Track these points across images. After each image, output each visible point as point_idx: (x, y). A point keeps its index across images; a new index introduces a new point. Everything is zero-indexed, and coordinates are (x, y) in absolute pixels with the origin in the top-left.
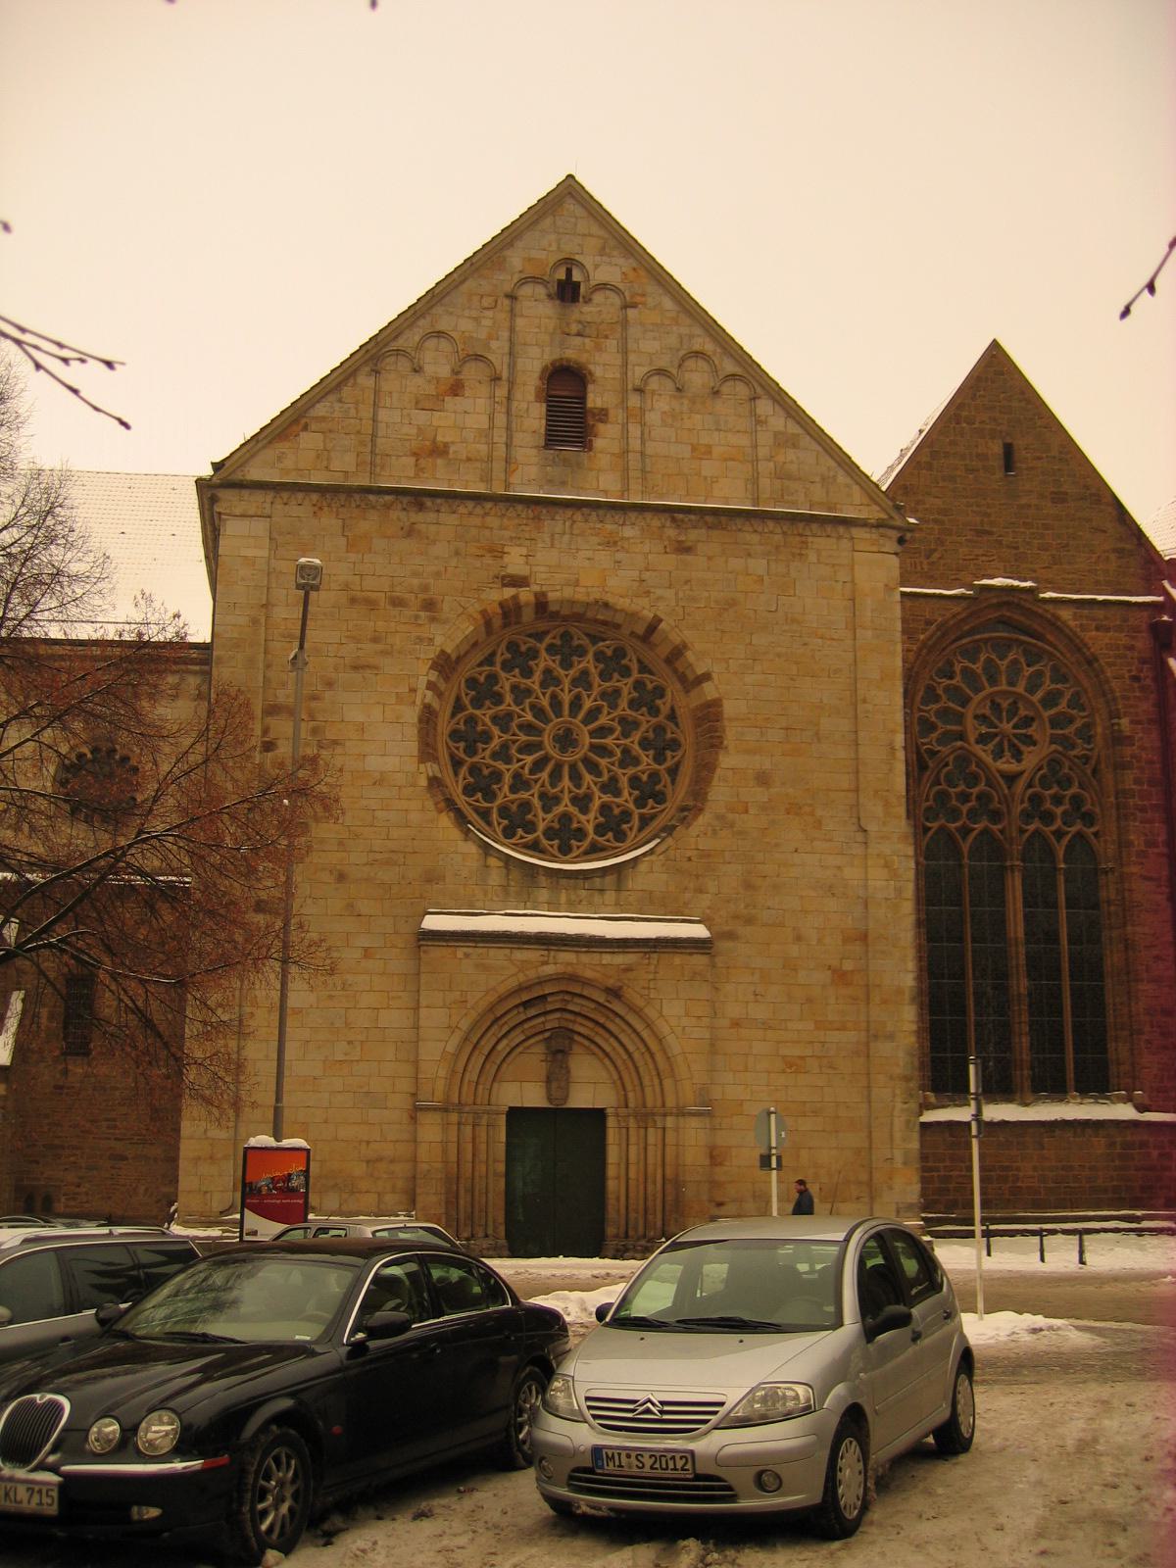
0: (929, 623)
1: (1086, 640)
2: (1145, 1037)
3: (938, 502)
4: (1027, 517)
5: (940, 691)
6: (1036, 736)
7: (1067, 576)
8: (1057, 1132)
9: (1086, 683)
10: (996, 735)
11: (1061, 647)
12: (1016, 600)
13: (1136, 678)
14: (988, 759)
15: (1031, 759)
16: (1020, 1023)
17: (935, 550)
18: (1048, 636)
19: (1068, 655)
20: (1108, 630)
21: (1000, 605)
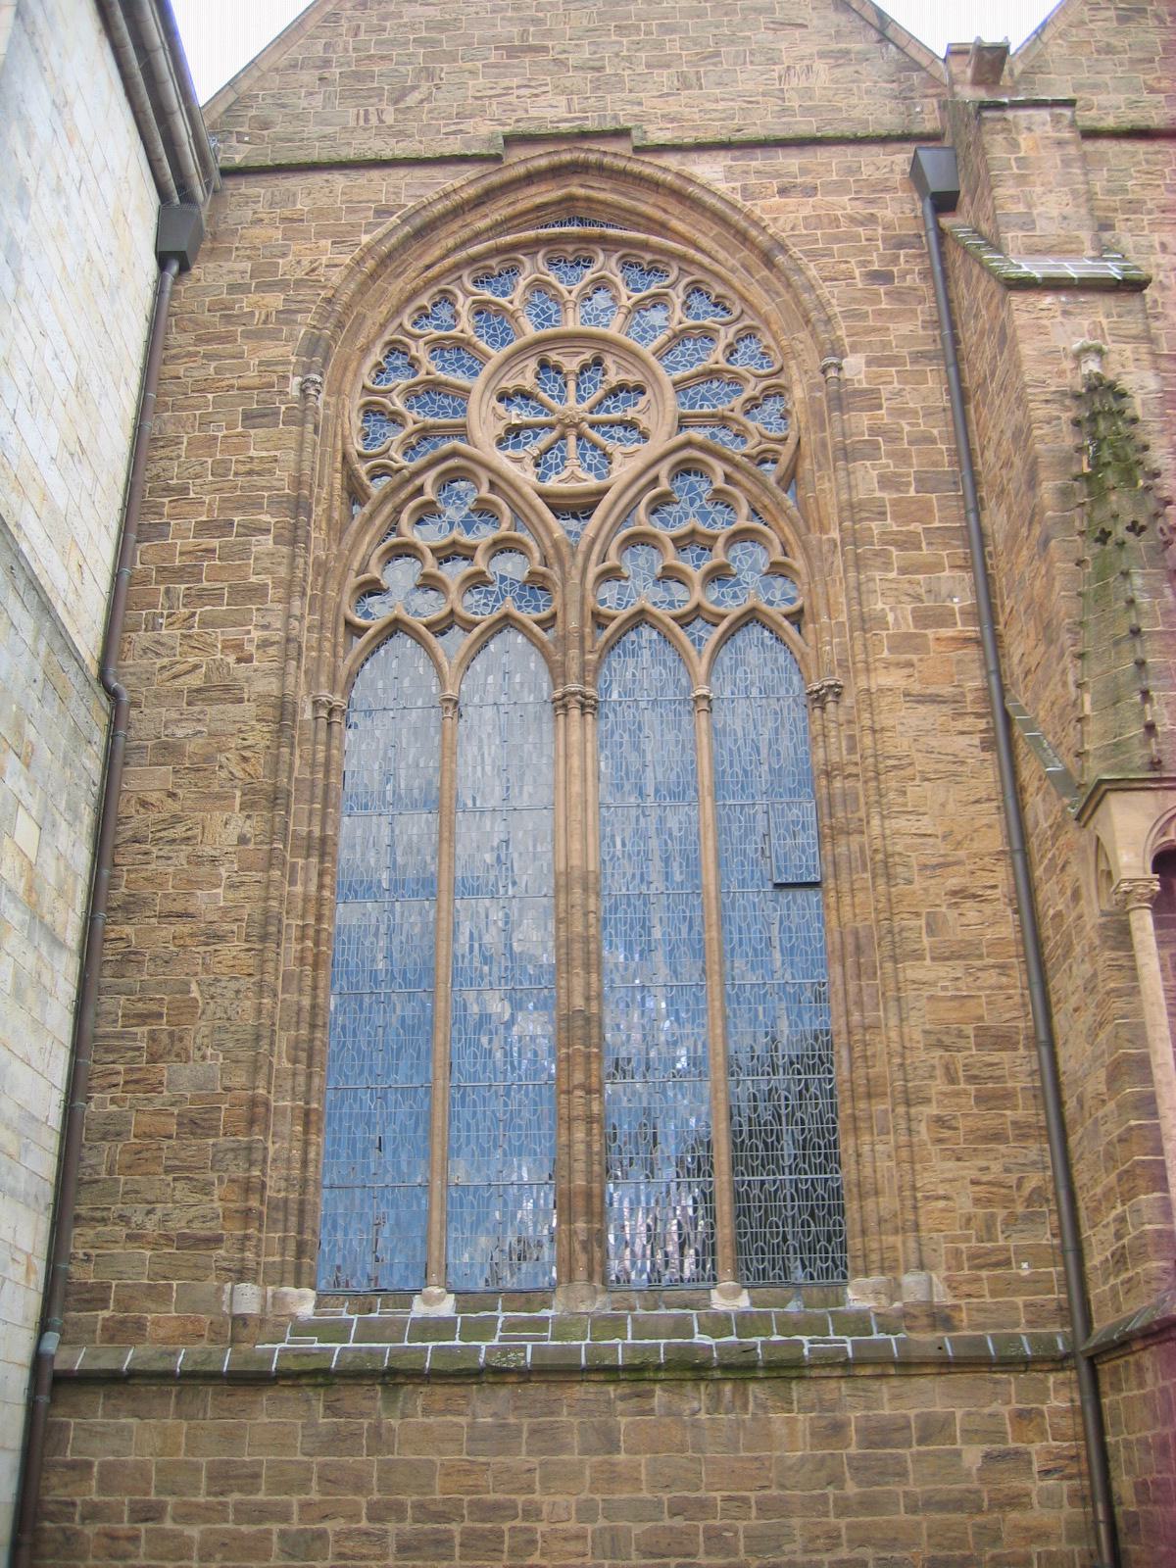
0: (383, 212)
1: (758, 212)
2: (933, 1110)
3: (430, 11)
4: (628, 18)
5: (419, 350)
6: (644, 422)
7: (714, 106)
8: (659, 1396)
9: (767, 306)
10: (551, 427)
11: (705, 242)
12: (593, 158)
13: (884, 277)
14: (525, 476)
15: (622, 471)
16: (569, 1092)
17: (414, 88)
18: (675, 224)
19: (722, 255)
20: (811, 191)
21: (556, 172)
